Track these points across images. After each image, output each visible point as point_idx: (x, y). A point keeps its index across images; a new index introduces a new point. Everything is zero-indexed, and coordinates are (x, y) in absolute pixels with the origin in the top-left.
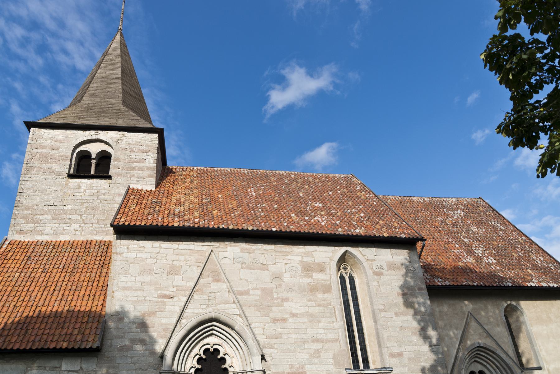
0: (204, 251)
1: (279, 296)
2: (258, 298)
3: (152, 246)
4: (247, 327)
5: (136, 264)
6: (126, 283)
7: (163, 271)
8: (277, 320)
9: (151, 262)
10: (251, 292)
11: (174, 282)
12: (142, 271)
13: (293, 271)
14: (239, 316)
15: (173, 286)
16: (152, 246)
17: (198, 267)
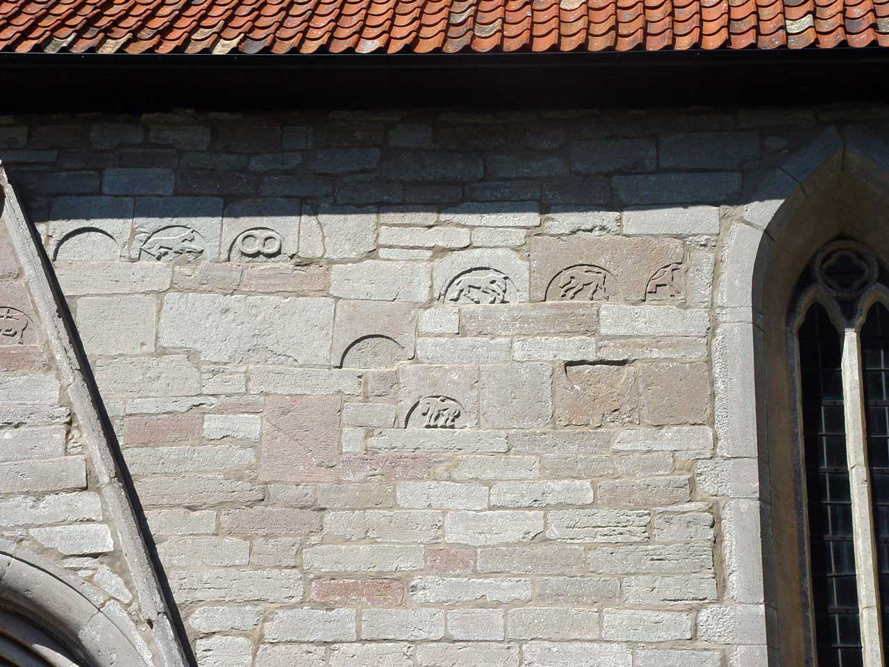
1: (373, 442)
2: (249, 455)
4: (145, 627)
8: (346, 590)
10: (213, 425)
13: (475, 294)
14: (111, 565)
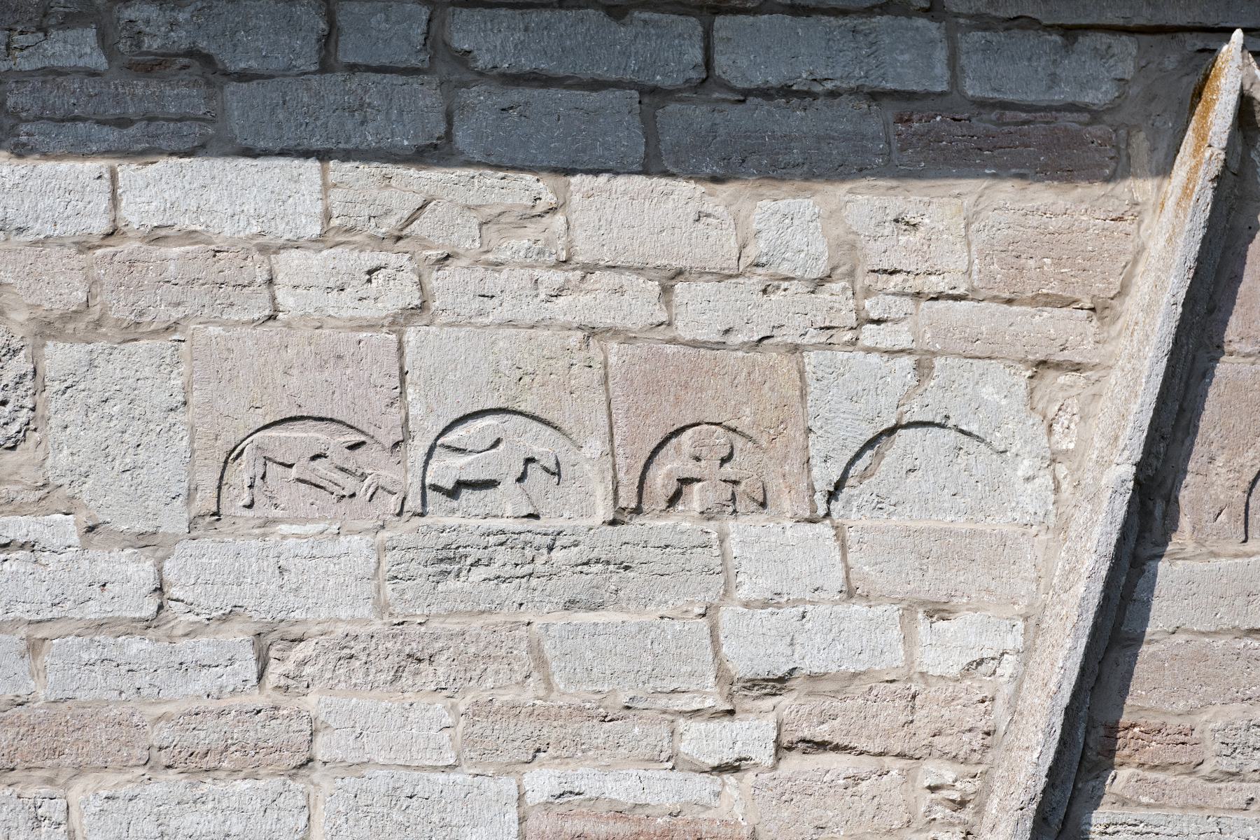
0: (1095, 115)
3: (328, 40)
5: (132, 331)
6: (34, 647)
7: (542, 444)
9: (344, 306)
11: (726, 616)
12: (234, 454)
15: (722, 676)
16: (328, 40)
17: (1042, 364)
